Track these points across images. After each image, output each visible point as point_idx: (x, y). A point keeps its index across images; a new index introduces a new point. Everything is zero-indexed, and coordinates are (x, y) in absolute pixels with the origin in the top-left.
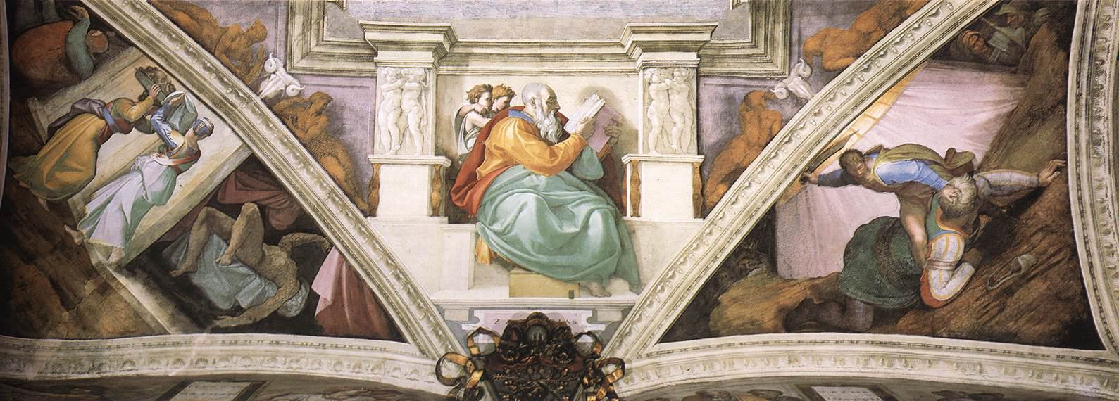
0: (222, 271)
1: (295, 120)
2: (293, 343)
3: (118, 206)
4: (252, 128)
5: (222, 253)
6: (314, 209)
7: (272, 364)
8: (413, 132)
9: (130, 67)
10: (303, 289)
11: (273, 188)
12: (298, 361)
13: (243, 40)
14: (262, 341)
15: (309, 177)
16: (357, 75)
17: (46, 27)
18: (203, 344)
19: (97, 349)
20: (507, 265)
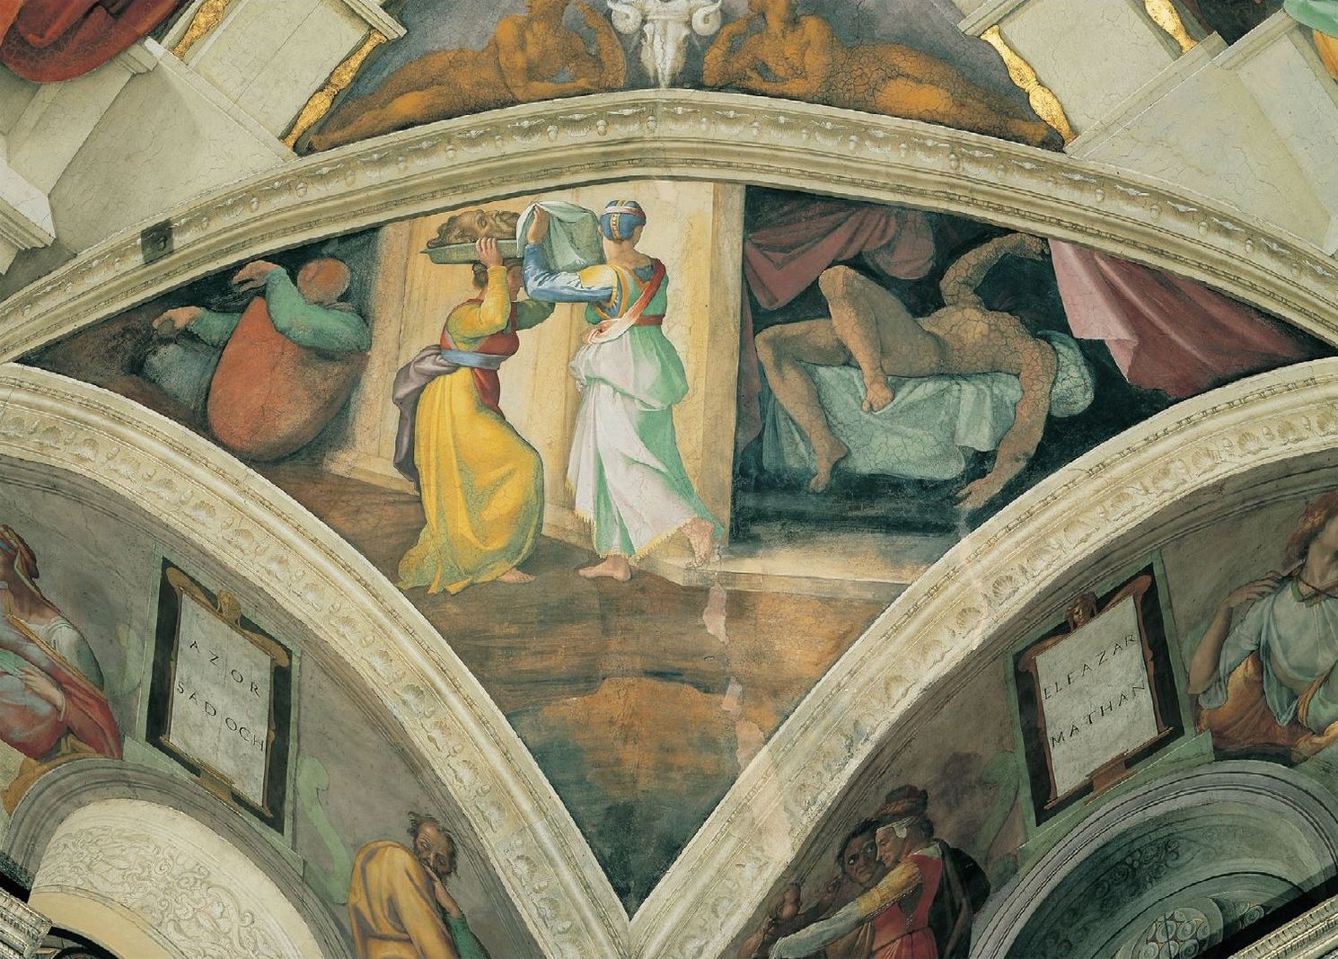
0: (892, 417)
1: (763, 70)
2: (1131, 450)
3: (621, 466)
5: (861, 391)
7: (1127, 506)
9: (412, 260)
11: (842, 215)
12: (1166, 473)
13: (538, 28)
15: (887, 149)
17: (229, 350)
18: (977, 555)
19: (826, 708)
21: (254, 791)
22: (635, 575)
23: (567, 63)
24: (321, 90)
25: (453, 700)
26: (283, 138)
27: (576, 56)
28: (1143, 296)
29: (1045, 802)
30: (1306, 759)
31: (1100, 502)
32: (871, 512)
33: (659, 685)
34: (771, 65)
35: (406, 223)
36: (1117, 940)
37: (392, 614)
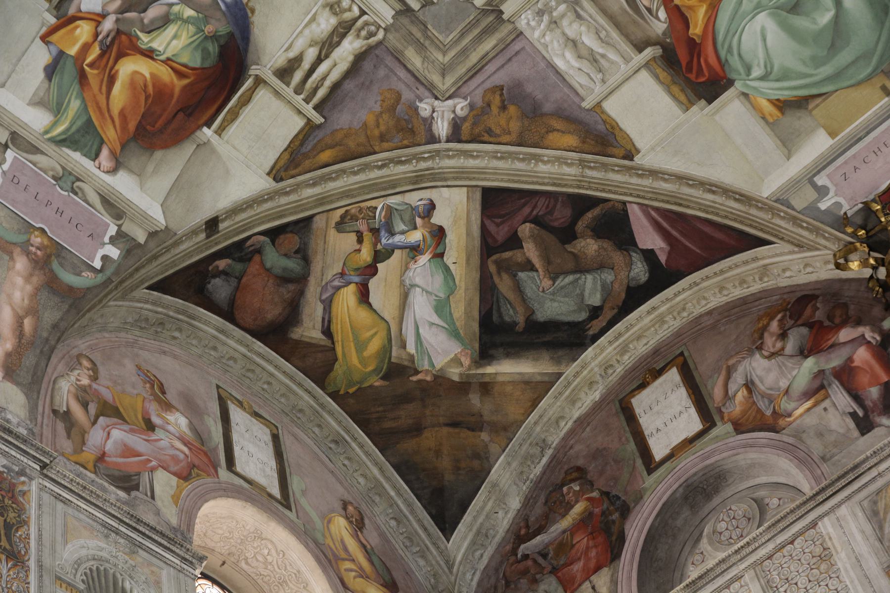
1: (489, 131)
2: (667, 299)
3: (427, 327)
4: (461, 170)
5: (539, 282)
6: (579, 187)
7: (666, 326)
8: (601, 51)
10: (634, 254)
14: (640, 317)
16: (503, 46)
18: (596, 356)
19: (529, 434)
20: (800, 104)
21: (276, 491)
22: (436, 377)
23: (398, 133)
24: (286, 150)
25: (354, 445)
26: (268, 174)
27: (402, 130)
28: (672, 227)
29: (650, 464)
30: (784, 429)
31: (653, 326)
32: (545, 339)
33: (451, 430)
34: (493, 129)
35: (325, 214)
36: (703, 524)
37: (322, 406)
